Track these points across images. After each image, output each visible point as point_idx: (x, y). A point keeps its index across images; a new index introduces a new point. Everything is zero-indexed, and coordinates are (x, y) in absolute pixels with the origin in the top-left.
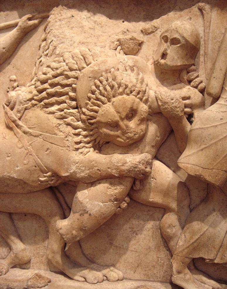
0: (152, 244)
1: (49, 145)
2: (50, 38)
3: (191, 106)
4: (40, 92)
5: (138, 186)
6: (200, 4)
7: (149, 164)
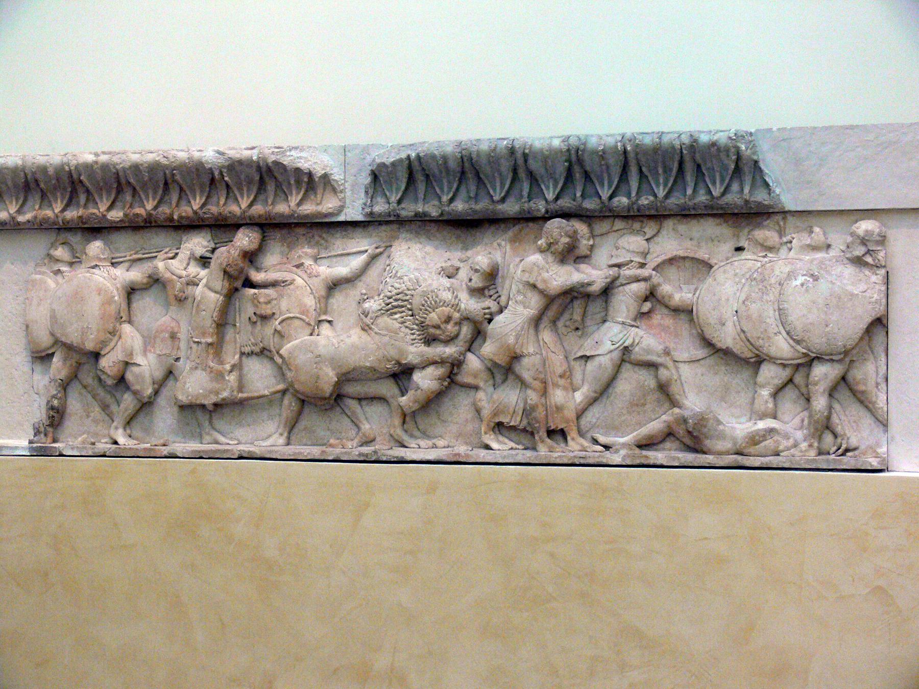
0: (469, 416)
1: (393, 342)
2: (393, 264)
3: (491, 314)
4: (388, 304)
5: (456, 370)
6: (499, 241)
7: (464, 355)
